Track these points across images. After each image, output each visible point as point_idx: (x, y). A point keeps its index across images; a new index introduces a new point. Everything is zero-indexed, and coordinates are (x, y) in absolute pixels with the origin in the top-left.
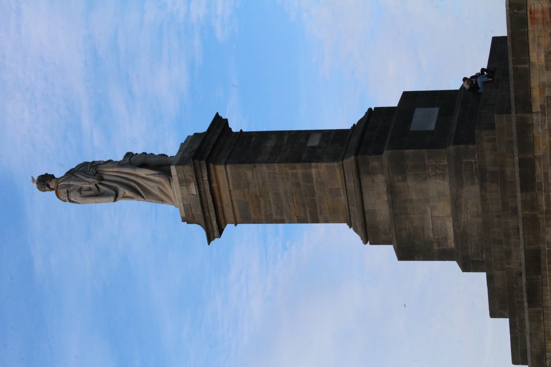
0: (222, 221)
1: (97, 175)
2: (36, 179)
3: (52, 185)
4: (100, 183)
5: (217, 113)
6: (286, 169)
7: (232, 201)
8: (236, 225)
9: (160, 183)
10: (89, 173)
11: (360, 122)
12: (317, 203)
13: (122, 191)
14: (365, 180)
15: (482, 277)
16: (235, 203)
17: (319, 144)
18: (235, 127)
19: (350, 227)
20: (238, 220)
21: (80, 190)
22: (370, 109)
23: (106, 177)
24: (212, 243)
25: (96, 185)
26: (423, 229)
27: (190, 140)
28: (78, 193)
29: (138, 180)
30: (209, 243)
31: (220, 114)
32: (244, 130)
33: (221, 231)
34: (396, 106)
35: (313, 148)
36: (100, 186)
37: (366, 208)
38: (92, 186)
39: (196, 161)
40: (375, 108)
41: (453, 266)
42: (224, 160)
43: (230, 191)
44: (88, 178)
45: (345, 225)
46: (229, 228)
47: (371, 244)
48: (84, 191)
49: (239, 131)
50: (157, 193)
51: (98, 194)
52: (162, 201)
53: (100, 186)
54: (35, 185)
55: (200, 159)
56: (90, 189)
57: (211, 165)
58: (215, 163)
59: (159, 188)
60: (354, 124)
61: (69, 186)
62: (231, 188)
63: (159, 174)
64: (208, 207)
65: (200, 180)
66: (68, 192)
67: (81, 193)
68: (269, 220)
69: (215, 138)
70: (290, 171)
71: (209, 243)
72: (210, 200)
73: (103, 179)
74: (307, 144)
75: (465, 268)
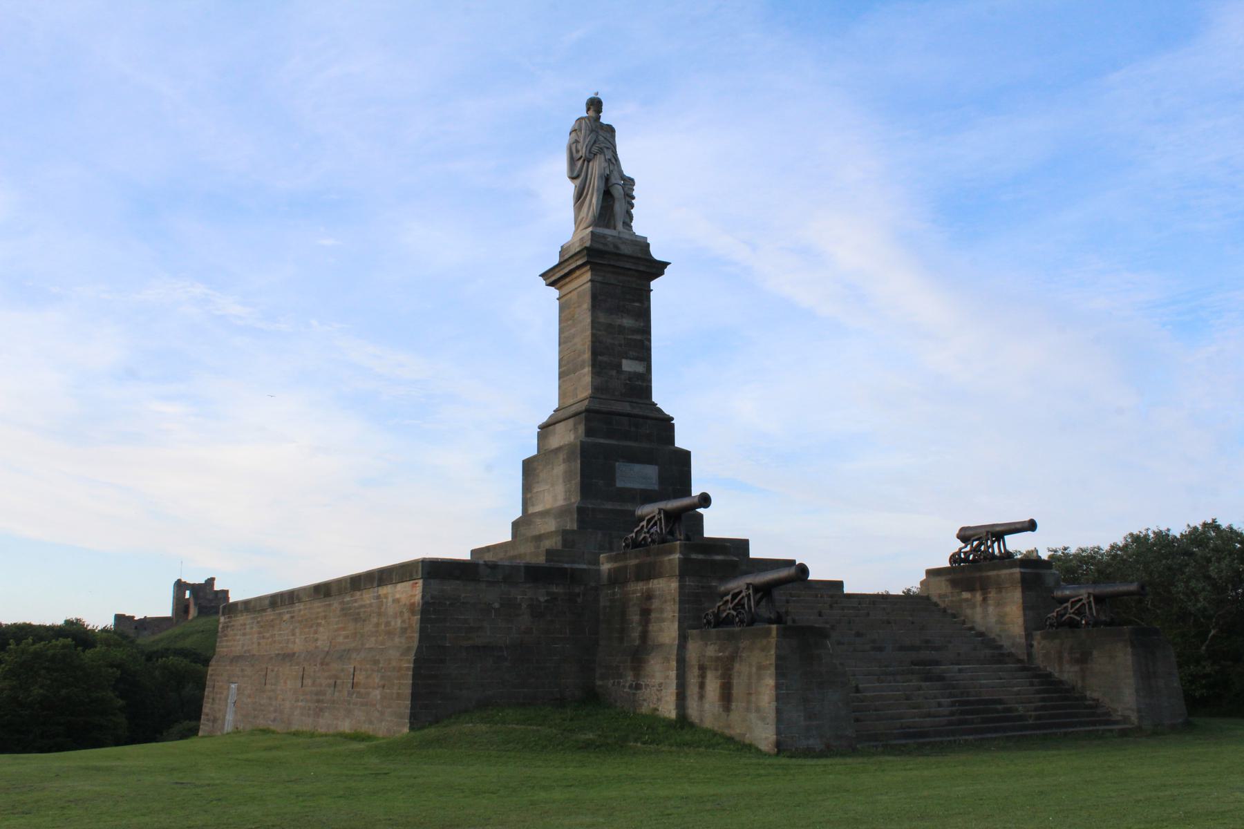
0: (559, 285)
2: (598, 96)
3: (592, 113)
4: (584, 160)
5: (669, 263)
6: (588, 343)
7: (570, 292)
8: (558, 299)
9: (587, 219)
10: (594, 147)
11: (660, 411)
12: (568, 377)
13: (578, 181)
14: (571, 421)
15: (509, 538)
16: (569, 296)
17: (626, 371)
18: (654, 284)
19: (554, 411)
20: (563, 300)
21: (577, 142)
22: (672, 419)
23: (591, 164)
24: (541, 278)
25: (582, 157)
26: (538, 482)
27: (642, 240)
28: (573, 140)
29: (589, 197)
30: (540, 276)
31: (668, 267)
32: (652, 293)
33: (551, 284)
34: (676, 445)
35: (620, 365)
36: (581, 161)
37: (557, 425)
38: (580, 154)
39: (585, 252)
40: (673, 424)
41: (517, 513)
42: (599, 279)
43: (576, 289)
44: (586, 147)
45: (556, 406)
46: (554, 293)
47: (538, 433)
48: (576, 147)
49: (651, 288)
50: (580, 218)
51: (572, 161)
52: (575, 224)
53: (581, 161)
54: (592, 95)
55: (588, 255)
56: (577, 151)
57: (588, 267)
58: (592, 269)
59: (583, 218)
60: (657, 404)
61: (581, 130)
62: (579, 289)
63: (594, 216)
64: (562, 269)
65: (575, 258)
66: (575, 130)
67: (573, 143)
68: (561, 331)
69: (628, 266)
70: (586, 346)
71: (540, 276)
72: (566, 270)
73: (589, 162)
75: (516, 525)
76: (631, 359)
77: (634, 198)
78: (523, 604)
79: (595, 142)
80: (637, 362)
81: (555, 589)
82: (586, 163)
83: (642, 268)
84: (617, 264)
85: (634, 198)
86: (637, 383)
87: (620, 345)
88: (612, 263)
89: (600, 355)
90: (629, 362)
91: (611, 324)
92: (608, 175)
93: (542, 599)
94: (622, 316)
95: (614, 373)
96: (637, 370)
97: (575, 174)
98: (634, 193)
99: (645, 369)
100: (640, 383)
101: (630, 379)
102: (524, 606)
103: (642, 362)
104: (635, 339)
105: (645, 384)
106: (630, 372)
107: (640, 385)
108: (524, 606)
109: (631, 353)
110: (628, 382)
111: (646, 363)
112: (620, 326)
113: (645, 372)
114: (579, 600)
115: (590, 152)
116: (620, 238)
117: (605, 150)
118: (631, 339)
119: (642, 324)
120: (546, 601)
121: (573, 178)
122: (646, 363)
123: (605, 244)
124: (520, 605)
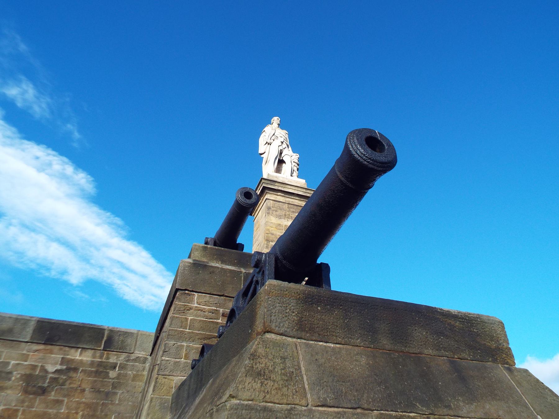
73: (270, 144)
78: (15, 373)
79: (274, 134)
81: (76, 355)
88: (280, 188)
91: (280, 224)
92: (281, 150)
93: (51, 368)
94: (288, 220)
102: (16, 375)
108: (16, 375)
114: (112, 374)
117: (279, 137)
120: (57, 371)
124: (10, 373)
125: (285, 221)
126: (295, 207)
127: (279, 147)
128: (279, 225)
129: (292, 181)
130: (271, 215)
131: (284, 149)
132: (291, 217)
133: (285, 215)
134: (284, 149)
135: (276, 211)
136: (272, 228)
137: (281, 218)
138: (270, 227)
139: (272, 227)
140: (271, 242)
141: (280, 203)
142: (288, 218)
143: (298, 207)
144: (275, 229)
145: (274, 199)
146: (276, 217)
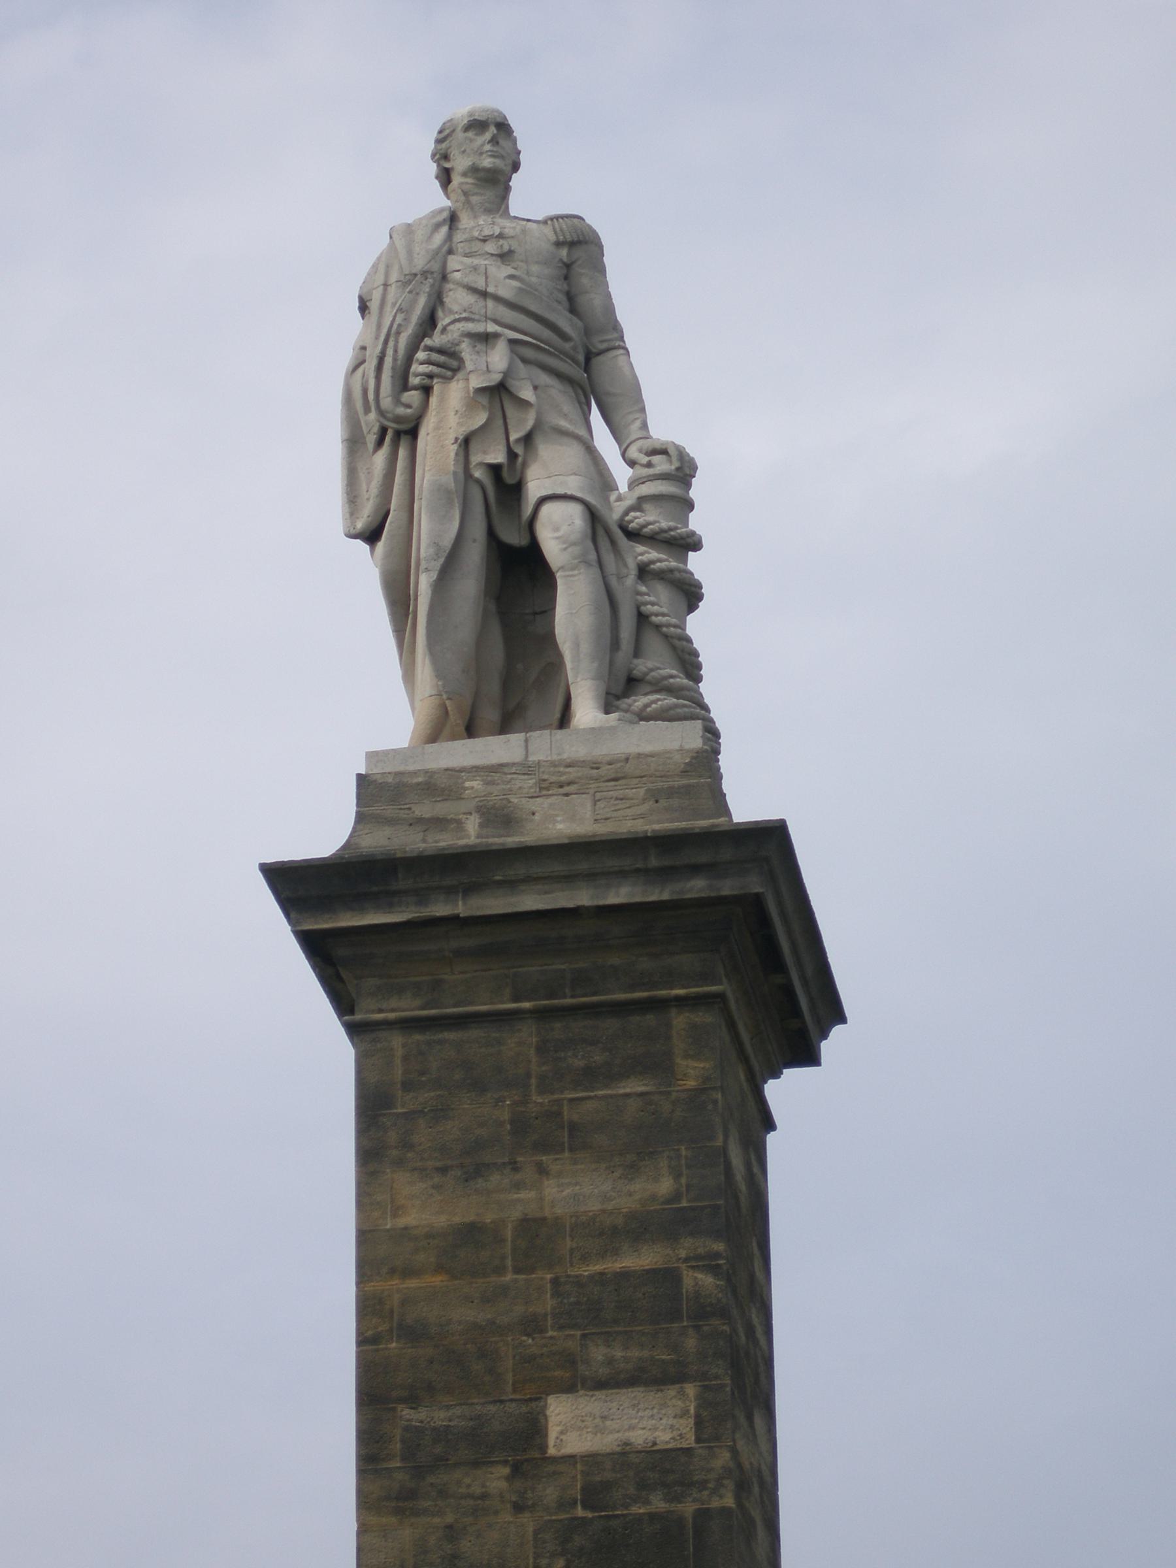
1: (413, 397)
10: (421, 355)
17: (571, 1459)
69: (530, 901)
73: (413, 433)
74: (569, 1388)
76: (601, 1385)
77: (692, 543)
79: (430, 322)
80: (637, 1393)
82: (402, 453)
83: (621, 894)
84: (461, 908)
85: (692, 543)
86: (638, 1510)
87: (532, 1325)
88: (440, 909)
89: (413, 1400)
90: (589, 1404)
92: (495, 469)
95: (496, 1479)
96: (639, 1438)
97: (360, 525)
98: (696, 522)
99: (687, 1427)
100: (658, 1503)
101: (593, 1496)
103: (671, 1391)
104: (625, 1275)
105: (688, 1508)
106: (592, 1460)
107: (653, 1517)
109: (598, 1353)
110: (580, 1512)
111: (691, 1390)
112: (530, 1226)
113: (690, 1441)
115: (402, 383)
116: (526, 769)
118: (601, 1279)
119: (665, 1186)
121: (372, 536)
122: (691, 1390)
123: (439, 823)
125: (518, 1186)
126: (611, 1025)
127: (473, 446)
128: (471, 1233)
129: (573, 773)
130: (400, 1163)
131: (528, 439)
132: (573, 1128)
133: (520, 1125)
134: (528, 439)
135: (440, 1113)
136: (413, 1283)
137: (478, 1171)
138: (393, 1271)
139: (408, 1272)
140: (406, 1412)
141: (475, 1033)
142: (545, 1146)
143: (635, 1019)
144: (438, 1280)
145: (407, 1006)
146: (443, 1170)
